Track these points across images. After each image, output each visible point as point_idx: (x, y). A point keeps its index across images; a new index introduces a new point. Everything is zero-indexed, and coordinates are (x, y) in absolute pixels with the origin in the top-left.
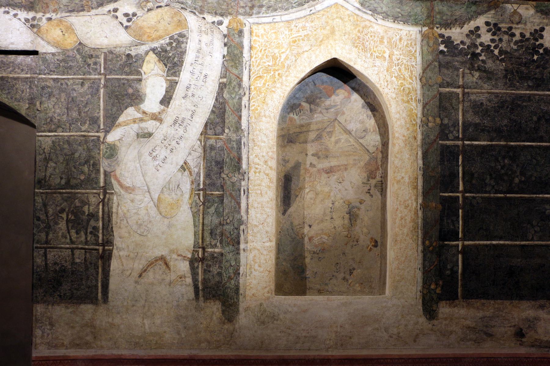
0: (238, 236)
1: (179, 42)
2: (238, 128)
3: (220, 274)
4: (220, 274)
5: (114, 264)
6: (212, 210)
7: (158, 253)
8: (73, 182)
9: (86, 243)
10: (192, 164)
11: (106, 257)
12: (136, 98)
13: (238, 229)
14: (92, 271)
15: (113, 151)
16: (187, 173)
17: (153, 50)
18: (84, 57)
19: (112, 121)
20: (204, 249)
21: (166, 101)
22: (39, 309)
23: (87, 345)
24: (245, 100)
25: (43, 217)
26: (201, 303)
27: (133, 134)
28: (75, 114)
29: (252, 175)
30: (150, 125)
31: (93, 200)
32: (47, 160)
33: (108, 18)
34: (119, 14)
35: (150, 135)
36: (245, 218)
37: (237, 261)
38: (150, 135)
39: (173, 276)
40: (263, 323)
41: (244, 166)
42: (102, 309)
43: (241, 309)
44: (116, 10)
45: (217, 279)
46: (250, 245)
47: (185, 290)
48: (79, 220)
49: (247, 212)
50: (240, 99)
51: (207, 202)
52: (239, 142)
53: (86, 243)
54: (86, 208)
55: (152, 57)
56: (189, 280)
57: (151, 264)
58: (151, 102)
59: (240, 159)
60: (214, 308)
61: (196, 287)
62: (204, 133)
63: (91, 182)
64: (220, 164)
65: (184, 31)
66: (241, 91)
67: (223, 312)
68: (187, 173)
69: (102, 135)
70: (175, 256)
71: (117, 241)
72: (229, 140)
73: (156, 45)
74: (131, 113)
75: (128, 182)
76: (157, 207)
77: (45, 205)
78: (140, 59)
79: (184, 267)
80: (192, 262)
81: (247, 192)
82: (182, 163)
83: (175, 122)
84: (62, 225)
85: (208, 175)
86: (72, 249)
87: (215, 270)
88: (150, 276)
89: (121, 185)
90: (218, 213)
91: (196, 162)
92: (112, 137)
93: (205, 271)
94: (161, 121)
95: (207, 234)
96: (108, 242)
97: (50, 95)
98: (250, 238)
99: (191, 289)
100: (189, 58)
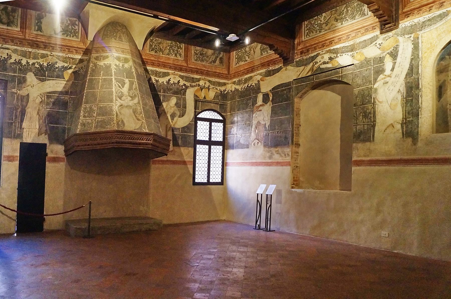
0: (418, 113)
1: (396, 48)
2: (418, 73)
3: (411, 128)
4: (411, 128)
5: (376, 128)
6: (409, 105)
7: (390, 123)
8: (364, 103)
9: (368, 122)
10: (401, 89)
11: (374, 126)
12: (383, 71)
13: (418, 110)
14: (369, 131)
15: (376, 90)
16: (400, 93)
17: (388, 53)
18: (367, 61)
19: (375, 80)
20: (406, 119)
21: (392, 70)
22: (354, 145)
23: (368, 156)
24: (420, 63)
25: (355, 116)
26: (405, 139)
27: (382, 83)
28: (364, 81)
29: (423, 89)
30: (388, 79)
31: (370, 108)
32: (357, 97)
33: (374, 46)
34: (377, 44)
35: (387, 82)
36: (421, 106)
37: (418, 122)
38: (387, 82)
39: (395, 130)
40: (427, 145)
41: (420, 87)
42: (372, 144)
43: (419, 140)
44: (376, 44)
45: (410, 130)
46: (423, 116)
47: (399, 135)
48: (366, 115)
49: (422, 104)
50: (419, 62)
51: (407, 102)
52: (418, 79)
53: (368, 122)
54: (368, 111)
55: (388, 55)
56: (401, 131)
57: (388, 127)
58: (388, 71)
59: (419, 84)
60: (410, 140)
61: (403, 133)
62: (406, 78)
63: (369, 102)
64: (411, 88)
65: (398, 44)
66: (419, 60)
67: (412, 142)
68: (400, 93)
69: (372, 86)
70: (396, 123)
71: (377, 121)
72: (415, 78)
73: (389, 51)
74: (381, 76)
75: (380, 100)
76: (390, 107)
77: (356, 112)
78: (384, 57)
79: (399, 126)
80: (402, 125)
81: (422, 96)
82: (398, 90)
83: (396, 76)
84: (361, 117)
85: (407, 93)
86: (364, 125)
87: (410, 126)
88: (388, 131)
89: (379, 101)
90: (411, 106)
91: (403, 89)
92: (375, 86)
93: (406, 127)
94: (391, 77)
95: (407, 114)
96: (375, 121)
97: (358, 76)
98: (423, 113)
99: (401, 134)
100: (400, 53)
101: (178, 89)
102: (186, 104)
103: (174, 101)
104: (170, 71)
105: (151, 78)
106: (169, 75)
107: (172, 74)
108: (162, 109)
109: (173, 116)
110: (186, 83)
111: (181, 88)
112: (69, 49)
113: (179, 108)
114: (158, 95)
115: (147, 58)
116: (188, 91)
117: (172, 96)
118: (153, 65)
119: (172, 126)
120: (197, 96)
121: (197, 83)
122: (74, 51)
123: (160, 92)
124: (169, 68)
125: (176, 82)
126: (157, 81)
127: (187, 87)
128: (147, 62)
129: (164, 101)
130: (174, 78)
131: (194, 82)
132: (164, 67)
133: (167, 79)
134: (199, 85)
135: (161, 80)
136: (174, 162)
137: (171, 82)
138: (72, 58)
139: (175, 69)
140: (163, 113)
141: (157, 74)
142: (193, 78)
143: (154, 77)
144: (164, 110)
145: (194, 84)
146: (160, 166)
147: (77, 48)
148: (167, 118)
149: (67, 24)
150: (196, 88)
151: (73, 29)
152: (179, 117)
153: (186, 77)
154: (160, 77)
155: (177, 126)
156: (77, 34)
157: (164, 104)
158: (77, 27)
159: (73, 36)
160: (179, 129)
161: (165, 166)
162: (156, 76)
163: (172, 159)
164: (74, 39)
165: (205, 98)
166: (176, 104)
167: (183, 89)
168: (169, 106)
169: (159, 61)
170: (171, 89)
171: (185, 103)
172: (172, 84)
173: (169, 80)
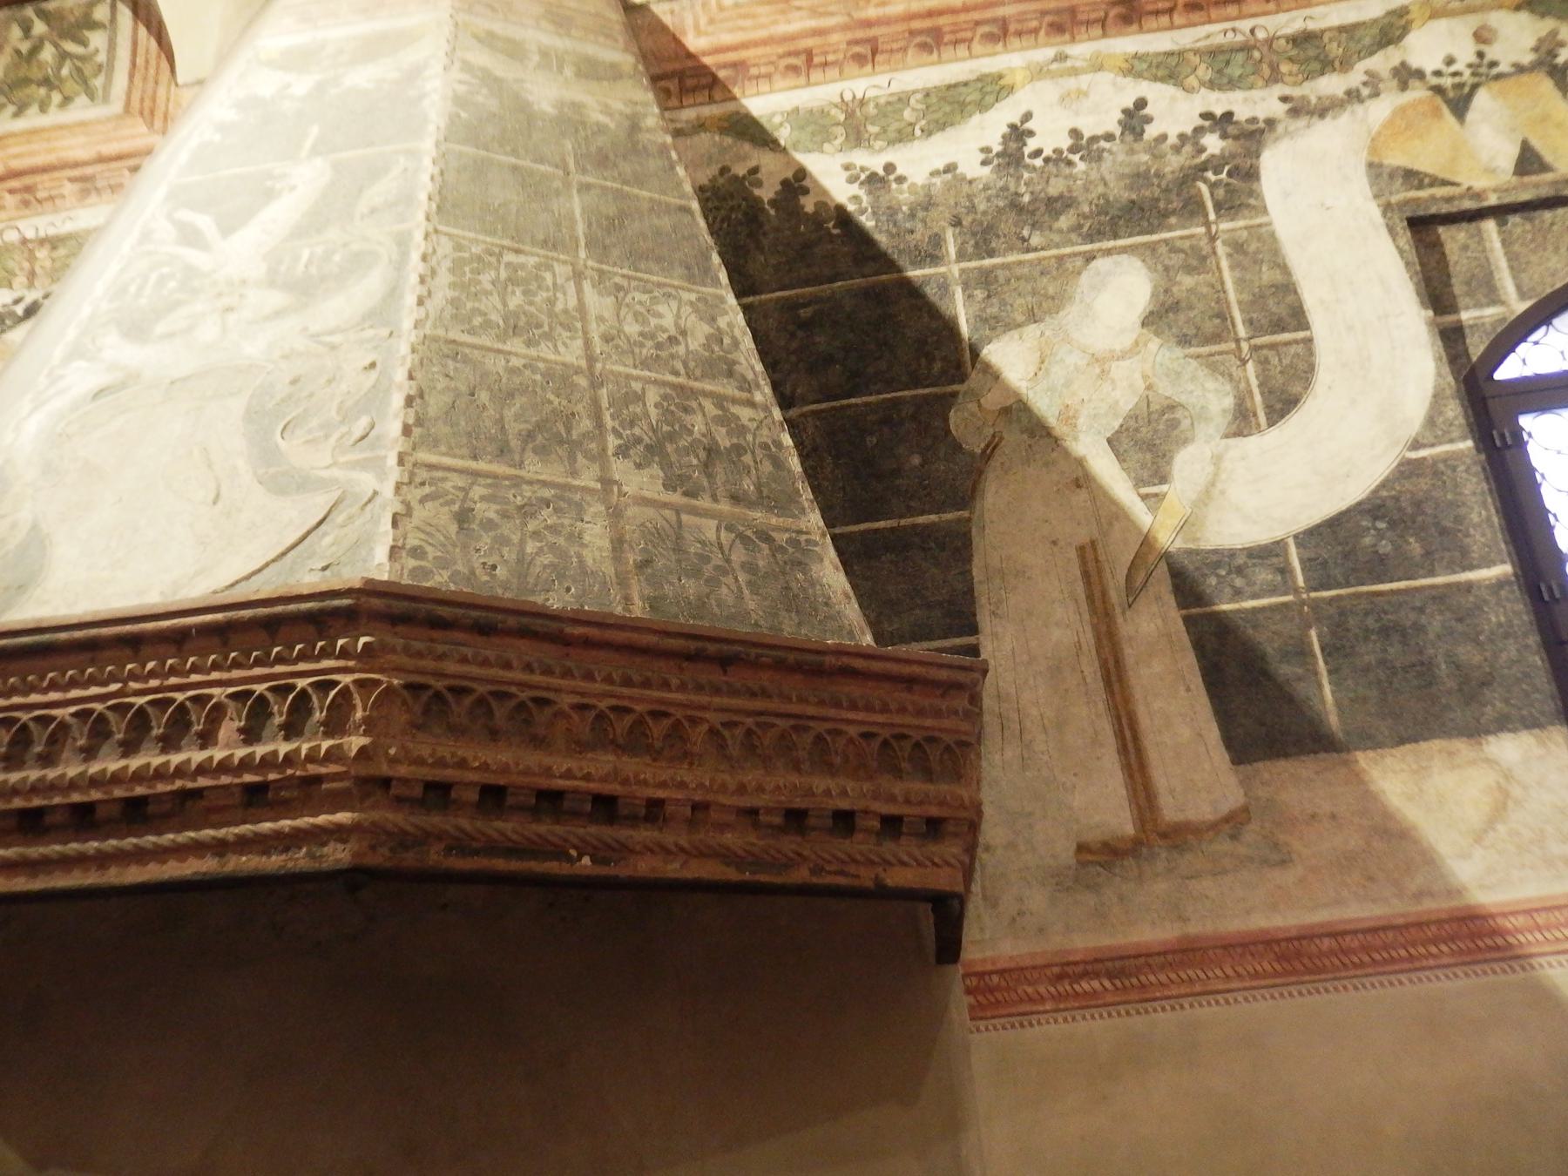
101: (1139, 178)
102: (1287, 287)
103: (1117, 292)
104: (1010, 60)
105: (801, 173)
106: (1011, 89)
107: (1038, 73)
108: (992, 401)
109: (1150, 440)
110: (1219, 103)
111: (1174, 163)
112: (28, 189)
113: (1216, 338)
114: (913, 292)
115: (727, 39)
116: (1277, 167)
117: (1090, 258)
118: (805, 61)
119: (1167, 538)
120: (1412, 177)
121: (1382, 62)
122: (69, 189)
123: (934, 258)
124: (991, 38)
125: (1102, 118)
126: (874, 182)
127: (1253, 136)
128: (735, 65)
129: (998, 324)
130: (1073, 96)
131: (1327, 65)
132: (925, 47)
133: (989, 128)
134: (1406, 75)
135: (917, 163)
136: (1296, 958)
137: (1049, 136)
138: (42, 242)
139: (1057, 28)
140: (1013, 437)
141: (855, 125)
142: (1303, 39)
143: (843, 158)
144: (1017, 412)
145: (1331, 85)
146: (1098, 1030)
147: (102, 160)
148: (1082, 480)
149: (25, 47)
150: (1379, 110)
151: (63, 56)
152: (1242, 422)
153: (1213, 53)
154: (903, 136)
155: (1233, 528)
156: (98, 82)
157: (1011, 358)
158: (97, 39)
159: (67, 100)
160: (1269, 553)
161: (1162, 1021)
162: (856, 137)
163: (1262, 921)
164: (81, 111)
165: (1528, 161)
166: (1162, 315)
167: (1215, 164)
168: (1075, 352)
169: (868, 24)
170: (1057, 205)
171: (1268, 275)
172: (1058, 159)
173: (1018, 134)
